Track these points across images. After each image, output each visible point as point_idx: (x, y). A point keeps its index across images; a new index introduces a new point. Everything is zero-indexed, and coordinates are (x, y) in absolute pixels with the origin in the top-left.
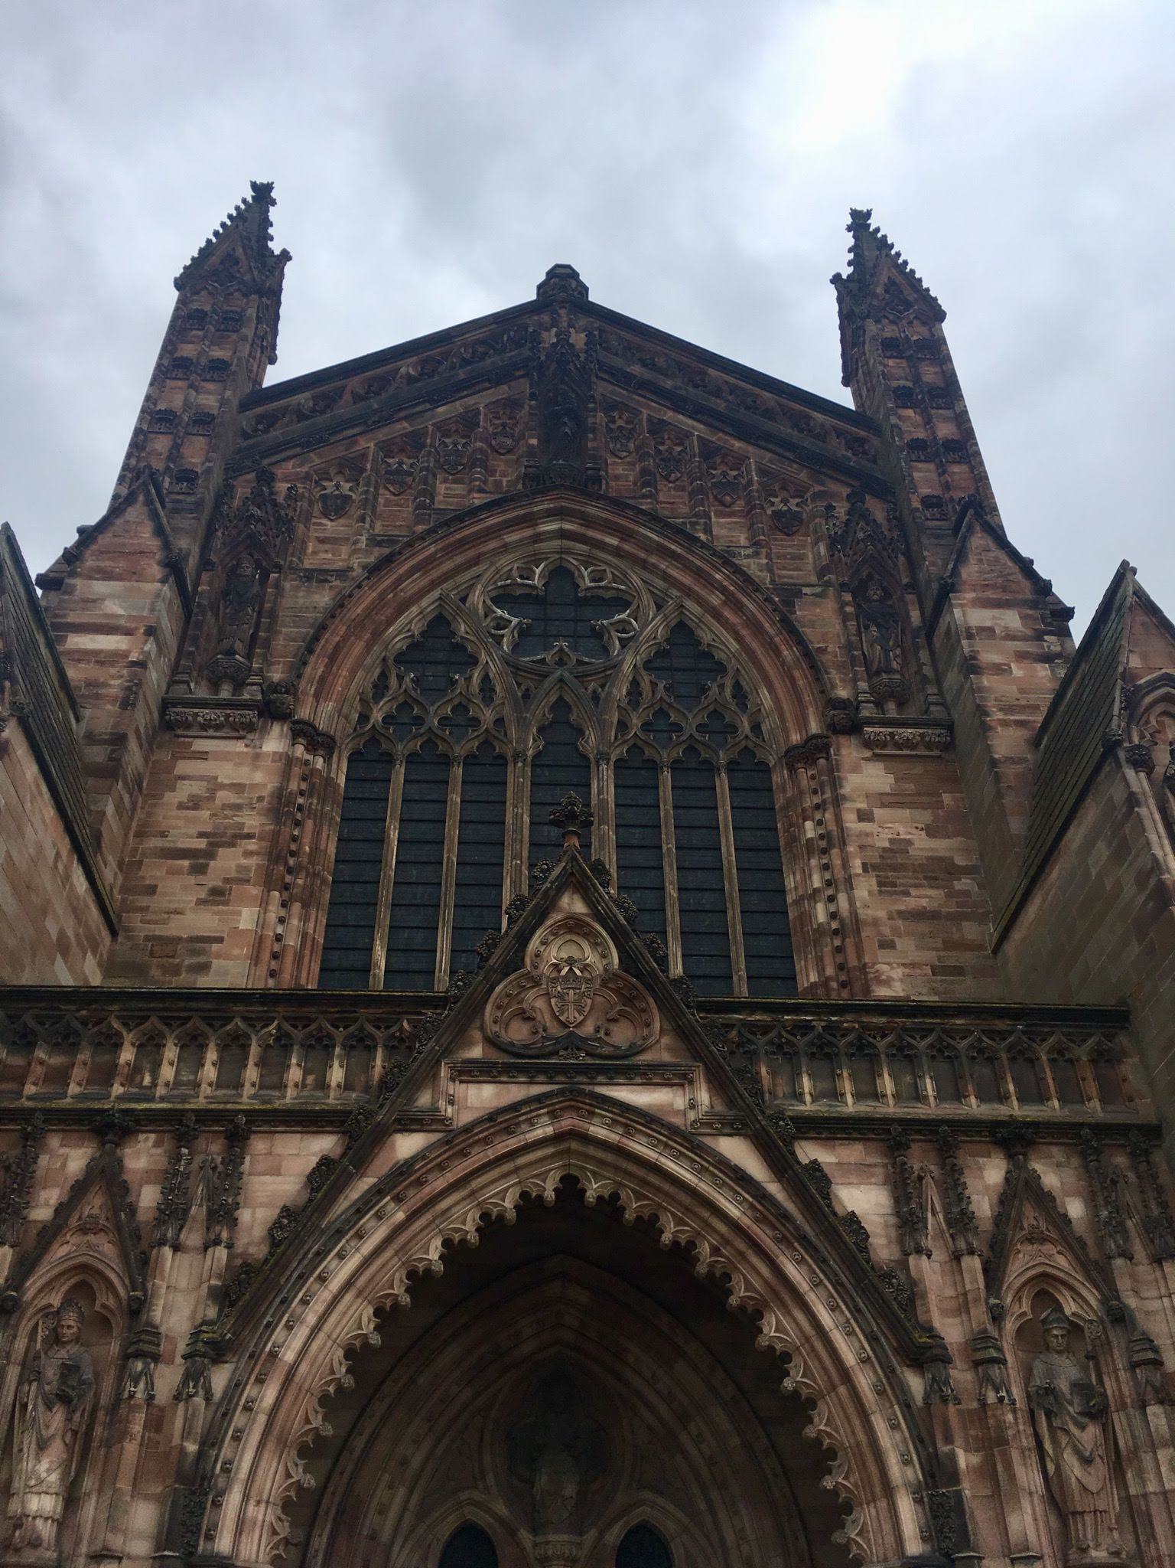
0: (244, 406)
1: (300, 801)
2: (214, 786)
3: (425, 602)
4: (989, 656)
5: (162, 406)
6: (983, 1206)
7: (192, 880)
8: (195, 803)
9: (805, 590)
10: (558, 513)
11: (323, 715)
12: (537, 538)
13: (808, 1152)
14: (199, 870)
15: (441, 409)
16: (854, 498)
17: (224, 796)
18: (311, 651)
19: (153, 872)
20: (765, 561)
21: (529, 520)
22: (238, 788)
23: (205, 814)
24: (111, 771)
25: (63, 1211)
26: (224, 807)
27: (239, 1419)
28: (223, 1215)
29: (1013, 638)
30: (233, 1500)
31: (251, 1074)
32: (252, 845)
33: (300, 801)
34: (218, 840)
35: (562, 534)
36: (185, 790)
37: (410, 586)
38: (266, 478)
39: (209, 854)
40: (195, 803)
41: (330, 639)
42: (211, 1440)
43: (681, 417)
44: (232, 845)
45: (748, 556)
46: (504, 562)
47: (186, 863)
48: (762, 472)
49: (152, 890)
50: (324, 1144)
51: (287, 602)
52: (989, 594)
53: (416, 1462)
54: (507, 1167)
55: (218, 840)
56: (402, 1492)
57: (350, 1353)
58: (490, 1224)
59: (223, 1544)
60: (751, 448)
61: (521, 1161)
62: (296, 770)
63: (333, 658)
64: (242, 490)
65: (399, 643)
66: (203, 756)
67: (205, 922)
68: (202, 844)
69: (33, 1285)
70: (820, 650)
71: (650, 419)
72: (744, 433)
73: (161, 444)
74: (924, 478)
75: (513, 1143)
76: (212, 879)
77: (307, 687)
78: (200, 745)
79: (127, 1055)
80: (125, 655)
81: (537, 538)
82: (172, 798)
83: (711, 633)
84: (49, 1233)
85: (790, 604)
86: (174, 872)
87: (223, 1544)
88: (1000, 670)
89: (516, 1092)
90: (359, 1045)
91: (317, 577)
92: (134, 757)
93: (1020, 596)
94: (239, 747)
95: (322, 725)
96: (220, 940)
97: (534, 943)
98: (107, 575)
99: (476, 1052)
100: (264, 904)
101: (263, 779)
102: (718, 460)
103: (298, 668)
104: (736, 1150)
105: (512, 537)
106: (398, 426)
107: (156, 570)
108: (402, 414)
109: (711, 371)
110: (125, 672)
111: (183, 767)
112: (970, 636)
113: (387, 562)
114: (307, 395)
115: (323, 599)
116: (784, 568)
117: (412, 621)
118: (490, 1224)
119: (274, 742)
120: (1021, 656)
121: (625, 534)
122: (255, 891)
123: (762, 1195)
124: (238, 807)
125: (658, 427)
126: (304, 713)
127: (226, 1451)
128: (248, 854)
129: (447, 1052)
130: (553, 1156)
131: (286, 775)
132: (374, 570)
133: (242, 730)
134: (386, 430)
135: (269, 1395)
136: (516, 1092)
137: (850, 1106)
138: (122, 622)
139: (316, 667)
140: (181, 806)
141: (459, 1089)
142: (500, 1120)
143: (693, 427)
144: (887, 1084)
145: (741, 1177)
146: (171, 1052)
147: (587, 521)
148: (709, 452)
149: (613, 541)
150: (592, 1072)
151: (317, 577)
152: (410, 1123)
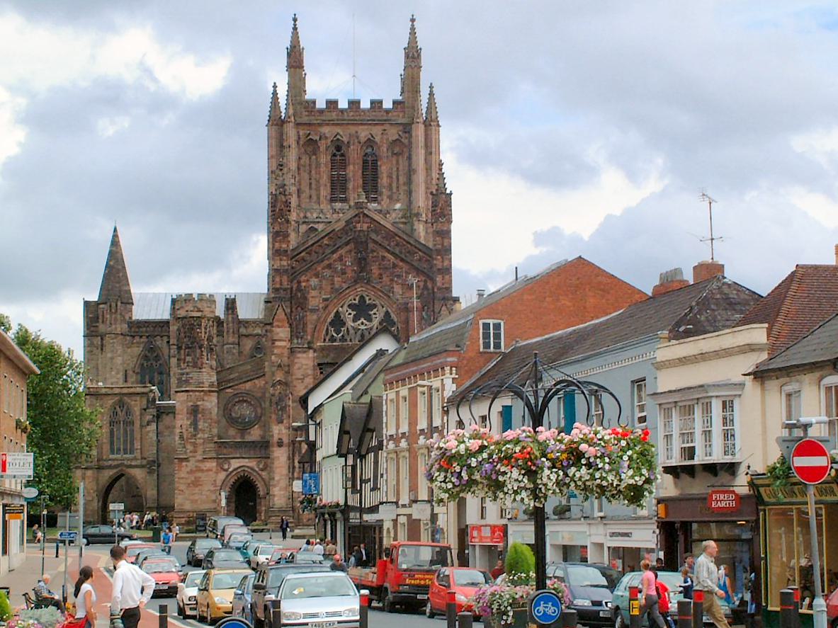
2: (302, 365)
5: (275, 267)
7: (301, 384)
8: (299, 369)
10: (362, 287)
14: (302, 382)
15: (335, 255)
16: (425, 281)
17: (304, 367)
18: (314, 332)
19: (295, 383)
21: (356, 289)
22: (307, 365)
23: (302, 370)
32: (310, 377)
34: (305, 376)
38: (299, 282)
39: (304, 379)
40: (299, 369)
43: (389, 255)
49: (295, 386)
51: (308, 318)
55: (305, 376)
64: (295, 286)
66: (299, 358)
68: (302, 377)
72: (402, 260)
74: (439, 279)
78: (299, 355)
80: (285, 346)
83: (393, 315)
86: (299, 383)
91: (313, 311)
94: (304, 355)
98: (278, 327)
103: (313, 336)
105: (352, 293)
106: (325, 262)
107: (287, 325)
111: (296, 361)
115: (315, 317)
119: (311, 354)
125: (384, 257)
133: (305, 352)
138: (284, 339)
148: (395, 266)
149: (373, 293)
151: (313, 311)
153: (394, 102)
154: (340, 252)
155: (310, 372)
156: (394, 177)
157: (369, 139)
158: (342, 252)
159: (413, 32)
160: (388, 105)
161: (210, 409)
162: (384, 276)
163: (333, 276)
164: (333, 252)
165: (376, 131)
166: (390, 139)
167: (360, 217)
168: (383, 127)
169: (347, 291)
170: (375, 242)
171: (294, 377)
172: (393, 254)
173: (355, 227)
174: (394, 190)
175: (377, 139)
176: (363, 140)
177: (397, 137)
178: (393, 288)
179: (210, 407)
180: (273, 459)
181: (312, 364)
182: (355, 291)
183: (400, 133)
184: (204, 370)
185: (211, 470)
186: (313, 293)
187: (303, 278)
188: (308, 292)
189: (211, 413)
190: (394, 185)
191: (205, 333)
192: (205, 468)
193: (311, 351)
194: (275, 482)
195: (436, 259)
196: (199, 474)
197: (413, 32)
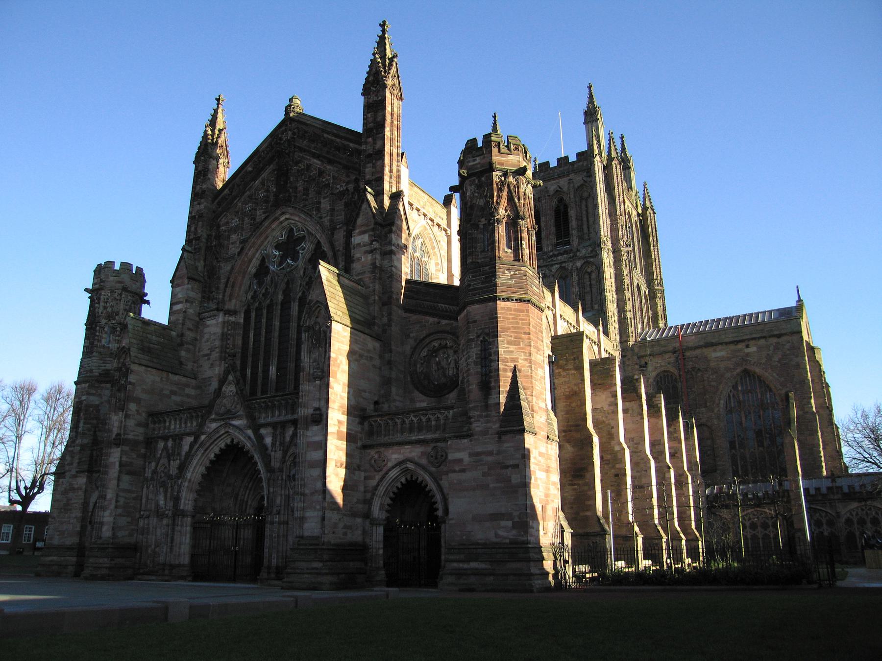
0: (213, 201)
1: (229, 332)
3: (257, 256)
4: (358, 255)
6: (288, 439)
9: (338, 227)
10: (283, 213)
11: (231, 305)
12: (281, 223)
13: (263, 431)
14: (209, 359)
17: (213, 337)
20: (329, 218)
21: (277, 219)
22: (214, 334)
23: (209, 343)
24: (181, 344)
25: (161, 454)
26: (213, 340)
27: (183, 488)
28: (179, 454)
29: (364, 246)
30: (183, 501)
31: (183, 425)
33: (229, 332)
35: (286, 219)
36: (206, 336)
37: (250, 253)
38: (219, 226)
41: (232, 280)
42: (179, 492)
43: (315, 160)
44: (214, 351)
45: (325, 217)
46: (274, 233)
47: (206, 358)
48: (334, 178)
50: (192, 439)
52: (363, 229)
53: (250, 486)
54: (220, 439)
55: (212, 350)
56: (248, 491)
57: (202, 475)
58: (221, 450)
59: (182, 507)
60: (332, 168)
61: (222, 437)
62: (226, 325)
63: (233, 287)
65: (254, 271)
66: (208, 326)
67: (209, 373)
68: (208, 352)
69: (159, 467)
70: (339, 250)
71: (307, 164)
72: (330, 162)
73: (193, 229)
75: (218, 435)
76: (211, 362)
77: (227, 298)
78: (209, 323)
79: (167, 424)
81: (281, 223)
82: (204, 339)
84: (160, 458)
85: (333, 234)
87: (182, 507)
88: (359, 259)
89: (219, 424)
90: (197, 416)
92: (189, 335)
93: (370, 227)
95: (232, 308)
96: (212, 377)
97: (224, 389)
99: (213, 416)
100: (220, 365)
101: (219, 330)
102: (325, 175)
104: (250, 432)
105: (273, 226)
106: (246, 194)
108: (247, 188)
109: (326, 135)
110: (182, 315)
111: (206, 330)
112: (354, 248)
113: (242, 249)
114: (227, 190)
116: (337, 216)
117: (256, 262)
118: (221, 450)
120: (367, 252)
121: (300, 217)
122: (218, 363)
123: (253, 442)
124: (215, 340)
126: (226, 307)
127: (181, 493)
128: (217, 353)
129: (208, 417)
130: (227, 436)
131: (223, 328)
132: (240, 253)
134: (243, 197)
135: (186, 484)
136: (219, 424)
137: (269, 420)
138: (182, 300)
139: (228, 290)
140: (205, 342)
141: (209, 425)
142: (216, 430)
143: (318, 164)
144: (277, 413)
145: (249, 438)
146: (173, 422)
147: (291, 215)
150: (229, 418)
151: (227, 260)
152: (203, 434)
153: (578, 155)
154: (263, 176)
155: (217, 343)
156: (585, 219)
157: (557, 191)
158: (265, 175)
159: (591, 97)
160: (573, 158)
161: (98, 406)
162: (310, 192)
163: (255, 210)
164: (254, 179)
165: (563, 182)
166: (576, 186)
167: (287, 125)
168: (569, 178)
169: (266, 224)
170: (301, 150)
171: (202, 353)
172: (318, 157)
173: (281, 139)
174: (586, 231)
175: (565, 189)
176: (551, 193)
177: (582, 182)
178: (319, 203)
179: (97, 403)
180: (106, 466)
181: (221, 331)
182: (277, 223)
183: (584, 179)
184: (94, 354)
185: (81, 489)
186: (234, 237)
187: (224, 220)
188: (228, 237)
189: (98, 411)
190: (585, 227)
191: (105, 308)
192: (76, 486)
193: (221, 314)
194: (106, 503)
195: (366, 143)
196: (71, 495)
197: (591, 97)
